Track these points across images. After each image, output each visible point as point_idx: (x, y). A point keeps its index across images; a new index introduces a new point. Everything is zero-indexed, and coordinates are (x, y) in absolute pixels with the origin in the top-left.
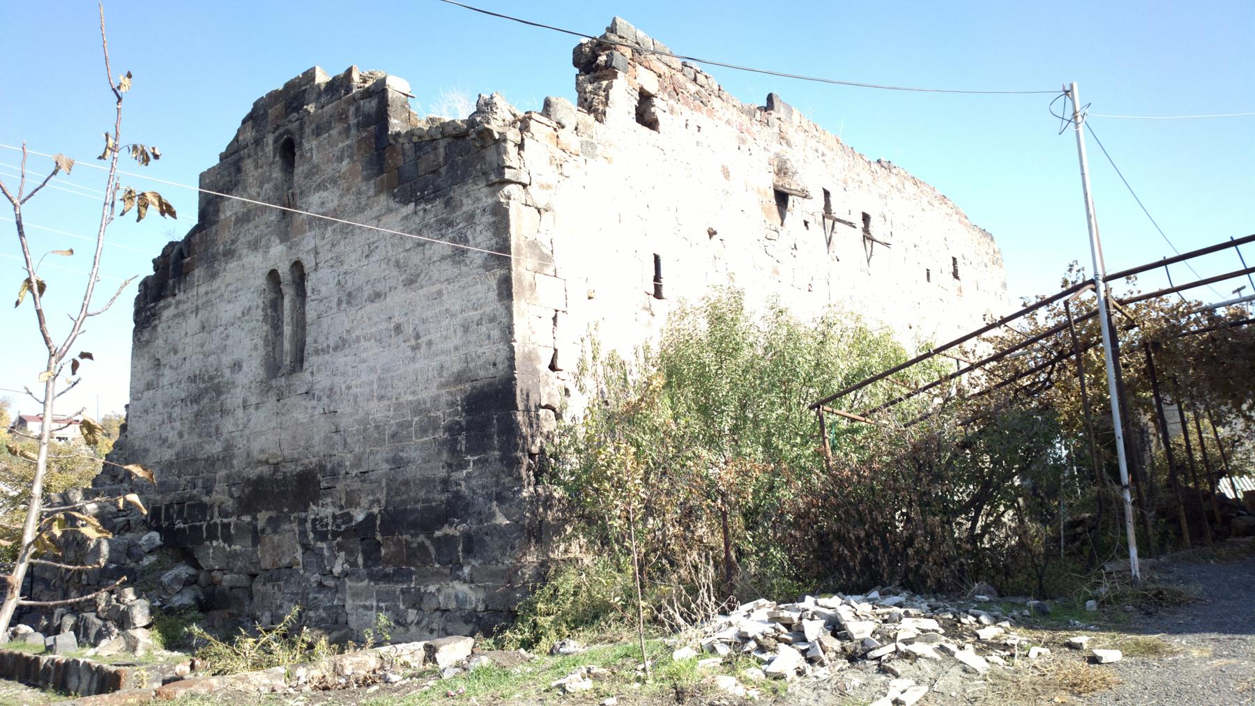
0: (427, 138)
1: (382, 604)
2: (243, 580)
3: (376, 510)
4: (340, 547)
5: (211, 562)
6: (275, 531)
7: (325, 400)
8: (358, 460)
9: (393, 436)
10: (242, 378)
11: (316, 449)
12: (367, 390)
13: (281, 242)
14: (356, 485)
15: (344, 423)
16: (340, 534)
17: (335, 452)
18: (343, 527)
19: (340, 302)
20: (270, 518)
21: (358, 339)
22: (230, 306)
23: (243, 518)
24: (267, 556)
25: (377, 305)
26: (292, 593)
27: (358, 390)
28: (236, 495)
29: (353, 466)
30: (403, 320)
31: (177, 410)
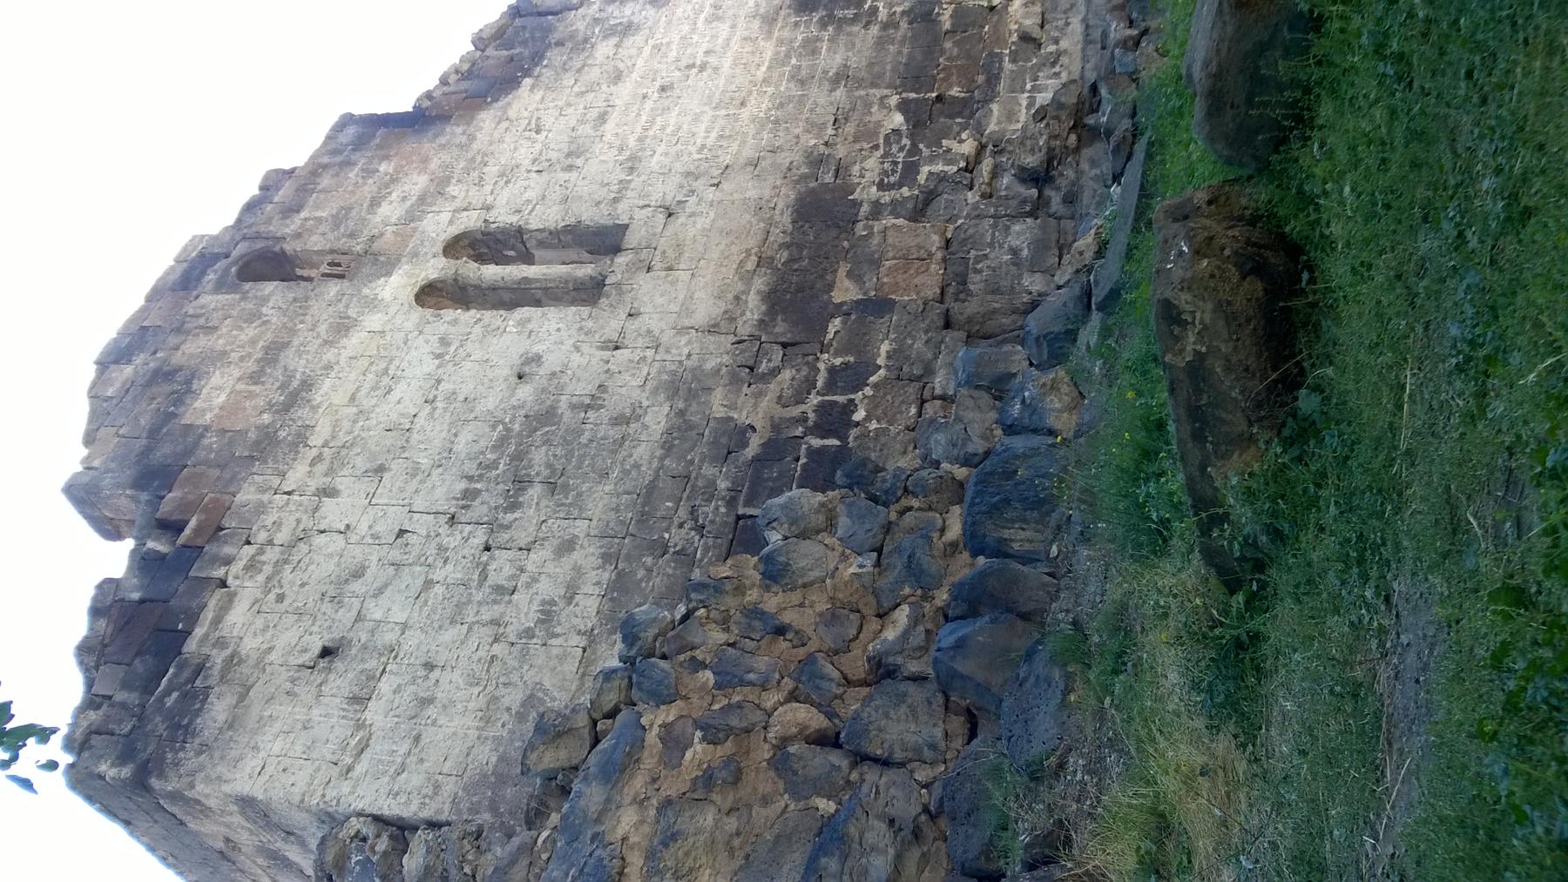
0: (466, 67)
1: (1028, 87)
3: (894, 100)
6: (876, 264)
7: (699, 185)
8: (814, 127)
9: (802, 83)
13: (389, 274)
14: (850, 129)
16: (914, 145)
18: (906, 141)
19: (570, 168)
21: (641, 140)
26: (994, 226)
27: (714, 135)
29: (818, 136)
30: (657, 84)
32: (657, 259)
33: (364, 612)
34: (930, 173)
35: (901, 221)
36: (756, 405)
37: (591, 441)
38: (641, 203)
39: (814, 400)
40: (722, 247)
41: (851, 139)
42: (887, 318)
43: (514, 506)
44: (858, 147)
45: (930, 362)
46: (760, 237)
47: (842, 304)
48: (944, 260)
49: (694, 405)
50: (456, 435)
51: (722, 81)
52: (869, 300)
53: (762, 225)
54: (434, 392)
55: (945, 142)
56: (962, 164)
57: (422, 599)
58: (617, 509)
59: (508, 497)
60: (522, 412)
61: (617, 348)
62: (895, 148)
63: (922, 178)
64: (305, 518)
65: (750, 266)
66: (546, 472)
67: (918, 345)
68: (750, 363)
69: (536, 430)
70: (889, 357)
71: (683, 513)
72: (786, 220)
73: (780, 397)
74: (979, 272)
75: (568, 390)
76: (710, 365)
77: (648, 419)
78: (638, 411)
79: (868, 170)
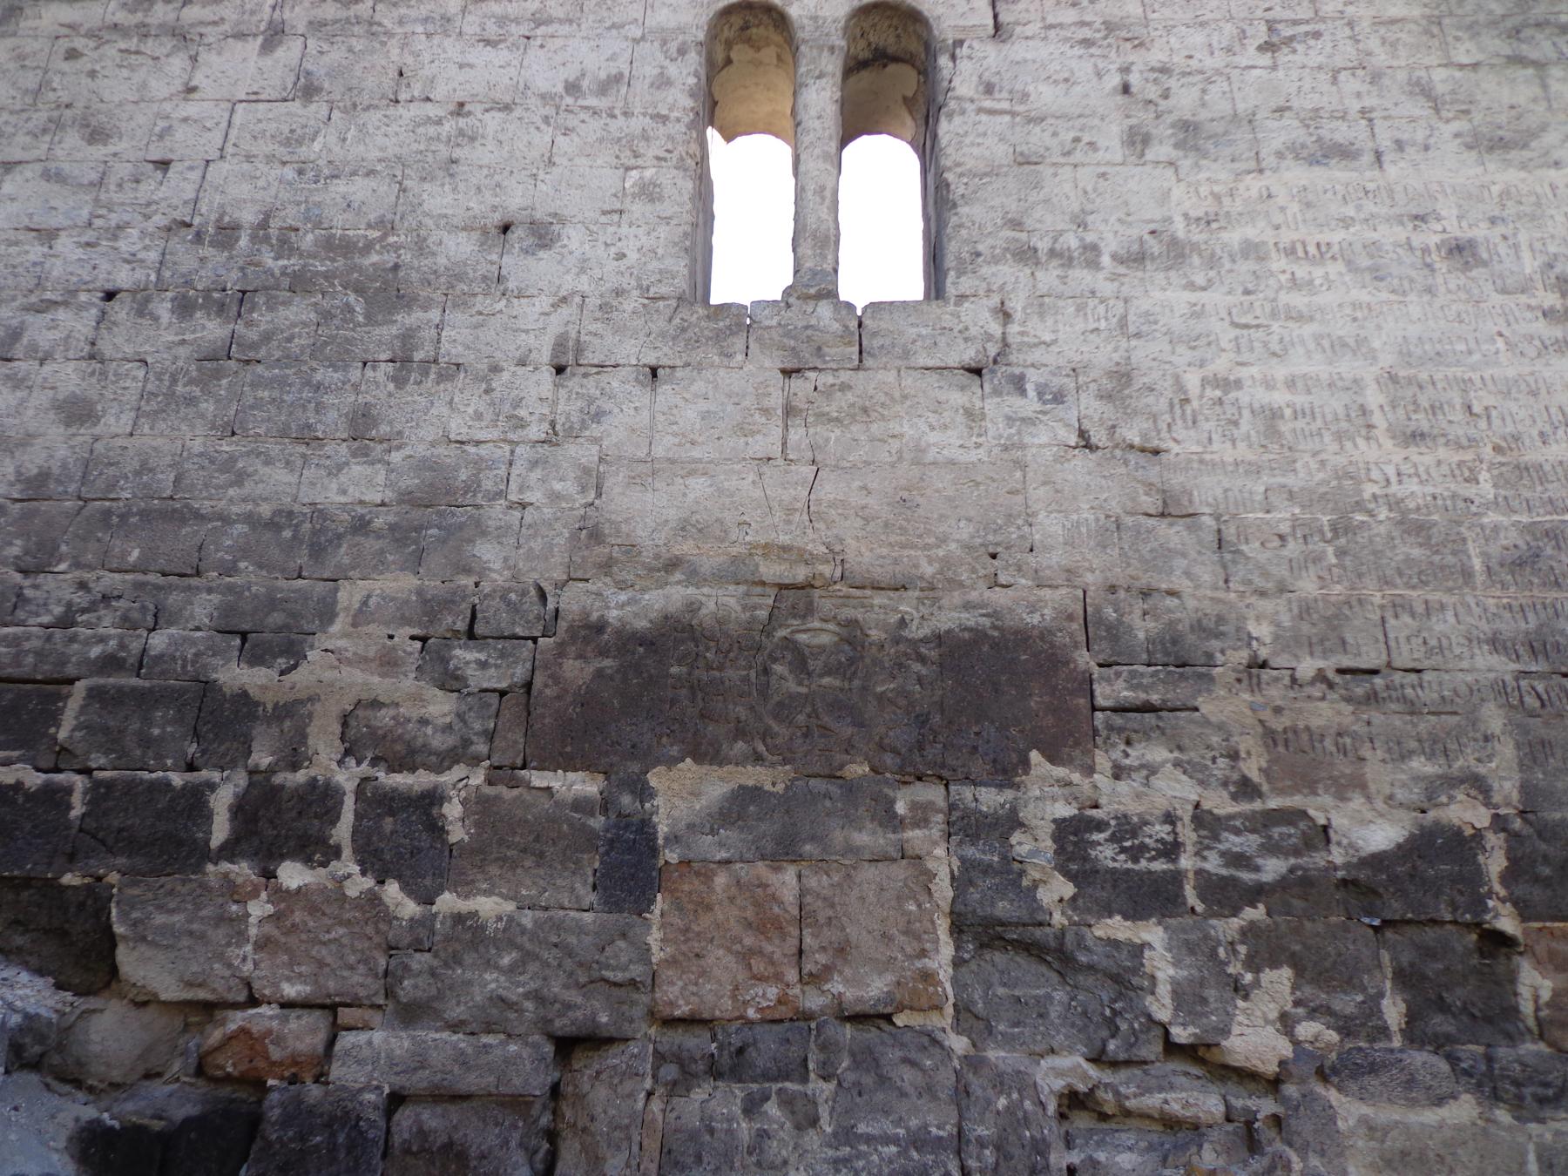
2: (522, 1063)
3: (1466, 813)
4: (1265, 950)
5: (245, 958)
6: (784, 851)
7: (1090, 407)
8: (1328, 626)
9: (1523, 563)
10: (536, 271)
11: (1055, 559)
12: (1335, 404)
14: (1326, 713)
15: (1206, 491)
16: (1257, 893)
17: (1184, 585)
18: (1273, 868)
19: (1138, 140)
20: (747, 796)
21: (1252, 250)
22: (481, 56)
23: (538, 779)
24: (720, 961)
25: (1338, 175)
26: (919, 1140)
27: (1279, 398)
28: (478, 679)
29: (1289, 641)
30: (1481, 232)
31: (78, 324)
32: (830, 379)
33: (19, 168)
34: (1138, 950)
35: (944, 890)
36: (361, 661)
37: (318, 387)
38: (1016, 305)
39: (346, 778)
40: (857, 499)
41: (1278, 724)
42: (591, 898)
43: (184, 308)
44: (1244, 744)
45: (437, 1014)
46: (881, 573)
47: (644, 792)
48: (807, 1016)
49: (378, 544)
50: (371, 173)
51: (1509, 369)
52: (654, 851)
53: (928, 570)
54: (477, 109)
55: (1279, 980)
56: (1181, 1034)
57: (21, 236)
58: (145, 468)
59: (208, 291)
60: (406, 256)
61: (560, 370)
62: (1247, 843)
63: (1116, 927)
64: (226, 27)
65: (772, 570)
66: (253, 335)
67: (493, 981)
68: (480, 629)
69: (359, 290)
70: (459, 919)
71: (110, 581)
72: (949, 618)
73: (376, 704)
74: (752, 1107)
75: (456, 317)
76: (487, 552)
77: (357, 469)
78: (379, 448)
79: (1152, 786)
